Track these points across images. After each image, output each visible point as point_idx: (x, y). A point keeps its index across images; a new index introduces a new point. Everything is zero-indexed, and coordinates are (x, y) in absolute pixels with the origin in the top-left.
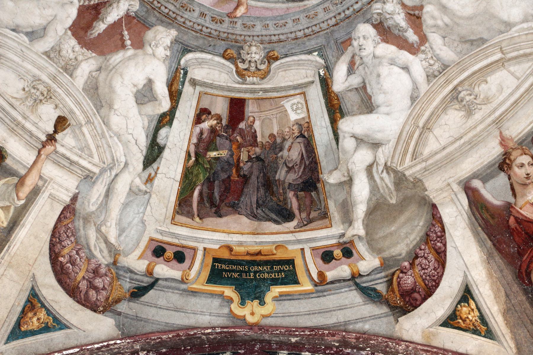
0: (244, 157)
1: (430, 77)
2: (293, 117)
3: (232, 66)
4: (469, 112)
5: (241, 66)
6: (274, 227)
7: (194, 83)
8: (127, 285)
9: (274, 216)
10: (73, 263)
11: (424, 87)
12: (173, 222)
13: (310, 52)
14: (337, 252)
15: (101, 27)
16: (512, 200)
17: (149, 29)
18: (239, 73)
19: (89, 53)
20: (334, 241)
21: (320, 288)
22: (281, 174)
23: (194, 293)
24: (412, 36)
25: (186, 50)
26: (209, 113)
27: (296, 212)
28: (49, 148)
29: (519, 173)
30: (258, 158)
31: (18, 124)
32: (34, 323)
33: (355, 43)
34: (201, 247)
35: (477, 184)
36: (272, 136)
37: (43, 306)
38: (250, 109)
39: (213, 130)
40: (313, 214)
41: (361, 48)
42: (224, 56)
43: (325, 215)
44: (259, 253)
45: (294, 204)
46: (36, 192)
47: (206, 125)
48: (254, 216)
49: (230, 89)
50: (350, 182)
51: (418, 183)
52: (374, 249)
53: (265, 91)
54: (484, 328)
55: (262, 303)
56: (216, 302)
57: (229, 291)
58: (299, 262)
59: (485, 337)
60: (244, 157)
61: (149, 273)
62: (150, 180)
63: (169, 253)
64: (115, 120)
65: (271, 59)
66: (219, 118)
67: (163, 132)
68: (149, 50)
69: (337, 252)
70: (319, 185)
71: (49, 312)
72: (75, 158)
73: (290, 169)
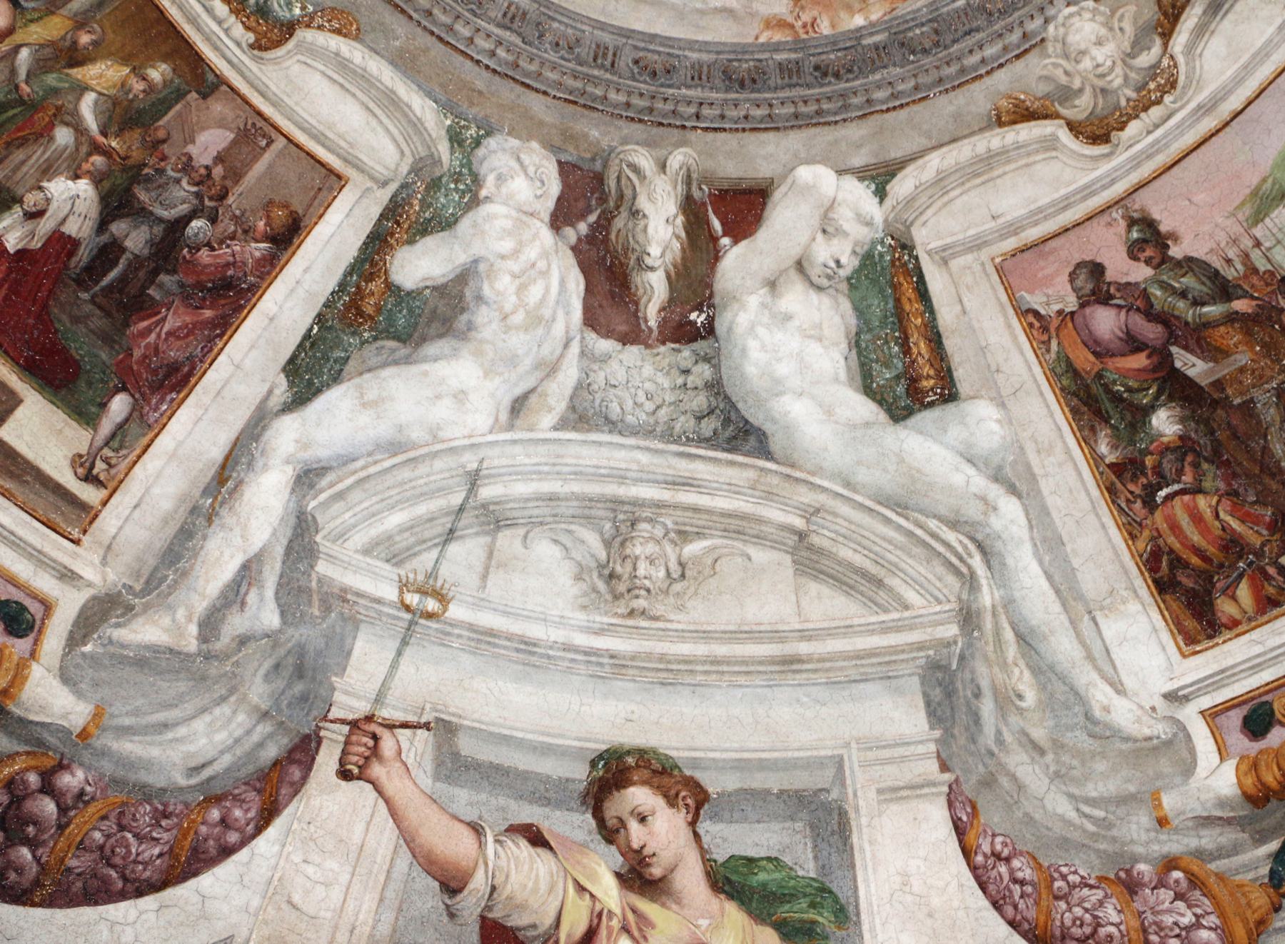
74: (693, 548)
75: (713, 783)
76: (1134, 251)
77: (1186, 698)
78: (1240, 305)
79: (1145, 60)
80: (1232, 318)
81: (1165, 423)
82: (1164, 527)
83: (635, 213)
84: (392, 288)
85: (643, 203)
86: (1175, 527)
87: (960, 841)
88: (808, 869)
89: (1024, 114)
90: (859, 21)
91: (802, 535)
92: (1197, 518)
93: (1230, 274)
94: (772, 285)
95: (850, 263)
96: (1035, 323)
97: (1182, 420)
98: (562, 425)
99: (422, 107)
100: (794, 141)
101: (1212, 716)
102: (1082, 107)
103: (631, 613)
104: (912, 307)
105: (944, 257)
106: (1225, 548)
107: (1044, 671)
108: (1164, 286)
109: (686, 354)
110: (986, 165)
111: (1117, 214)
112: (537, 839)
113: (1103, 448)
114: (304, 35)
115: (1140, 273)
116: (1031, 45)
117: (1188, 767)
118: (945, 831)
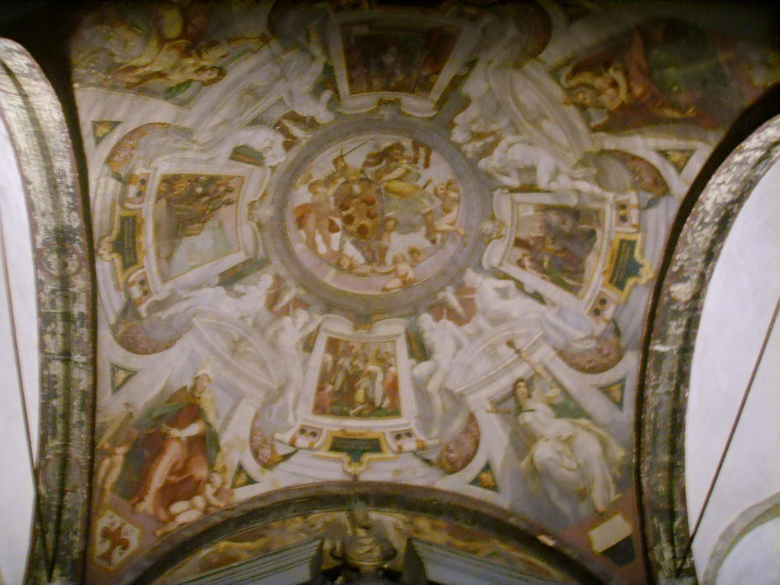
0: (550, 247)
1: (517, 132)
2: (531, 212)
3: (494, 241)
4: (544, 117)
5: (494, 236)
6: (598, 243)
7: (500, 264)
8: (611, 337)
9: (592, 240)
10: (591, 362)
11: (524, 137)
12: (582, 298)
13: (492, 196)
14: (622, 212)
15: (460, 310)
16: (606, 110)
17: (464, 284)
18: (500, 237)
19: (474, 319)
20: (614, 212)
21: (642, 229)
22: (566, 228)
23: (626, 302)
24: (490, 139)
25: (480, 265)
26: (520, 260)
27: (590, 227)
28: (523, 354)
29: (588, 101)
30: (554, 239)
31: (506, 367)
32: (617, 394)
33: (490, 170)
34: (600, 289)
35: (592, 125)
36: (541, 227)
37: (609, 386)
38: (522, 235)
39: (532, 260)
40: (595, 217)
41: (494, 167)
42: (487, 244)
43: (597, 212)
44: (612, 257)
45: (585, 227)
46: (546, 369)
47: (527, 262)
48: (588, 252)
49: (508, 245)
50: (579, 193)
51: (587, 155)
52: (624, 191)
53: (512, 224)
54: (686, 154)
55: (642, 266)
56: (635, 292)
57: (631, 282)
58: (622, 236)
59: (692, 155)
60: (550, 247)
61: (608, 322)
62: (553, 304)
63: (599, 306)
64: (515, 314)
65: (493, 218)
66: (525, 255)
67: (527, 288)
68: (477, 286)
69: (622, 212)
70: (577, 209)
71: (614, 384)
72: (531, 342)
73: (563, 223)
74: (244, 105)
75: (204, 88)
76: (229, 199)
77: (154, 171)
78: (208, 212)
79: (256, 219)
80: (208, 209)
81: (199, 190)
82: (184, 181)
83: (303, 129)
84: (328, 89)
85: (302, 132)
86: (182, 183)
87: (161, 123)
88: (178, 97)
89: (264, 195)
90: (299, 181)
91: (230, 123)
92: (182, 187)
93: (214, 213)
94: (272, 142)
95: (264, 155)
96: (232, 178)
97: (197, 193)
98: (282, 98)
99: (348, 112)
100: (291, 159)
101: (148, 175)
102: (257, 205)
103: (243, 90)
104: (250, 160)
105: (252, 170)
106: (173, 189)
107: (176, 150)
108: (220, 201)
109: (274, 122)
110: (261, 184)
111: (236, 200)
112: (223, 56)
113: (203, 178)
114: (375, 106)
115: (225, 198)
116: (273, 203)
117: (145, 166)
118: (164, 122)
